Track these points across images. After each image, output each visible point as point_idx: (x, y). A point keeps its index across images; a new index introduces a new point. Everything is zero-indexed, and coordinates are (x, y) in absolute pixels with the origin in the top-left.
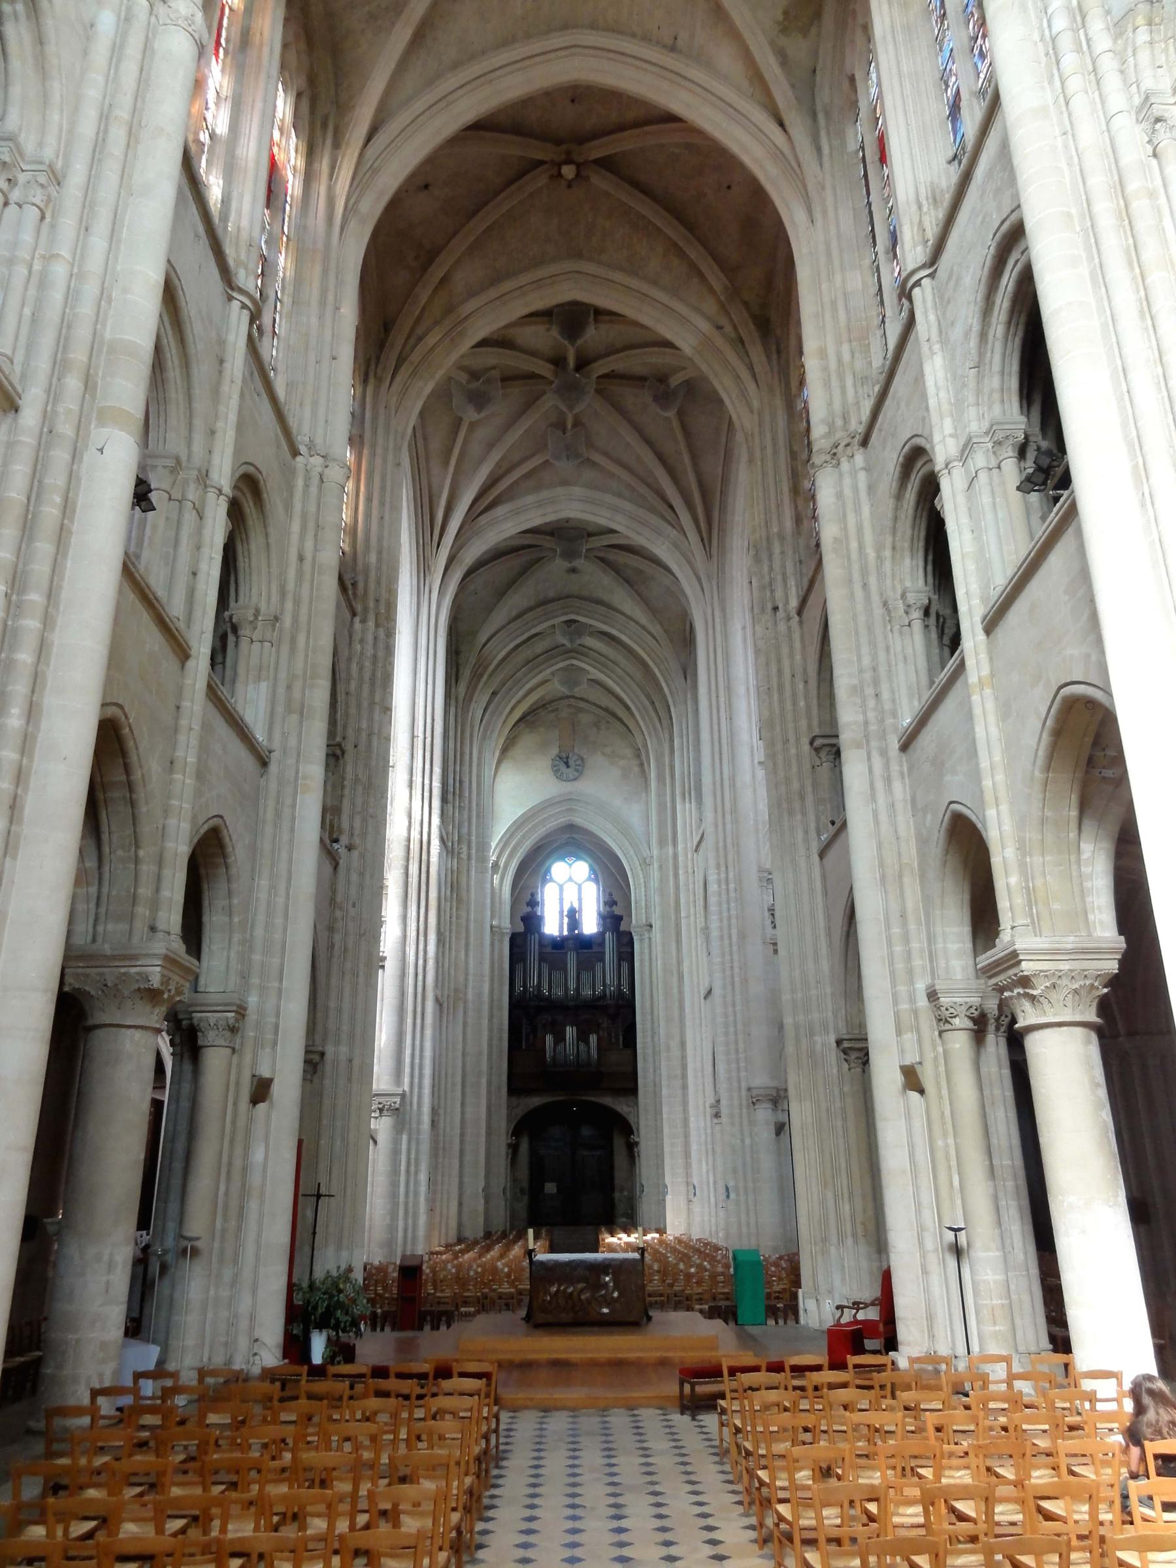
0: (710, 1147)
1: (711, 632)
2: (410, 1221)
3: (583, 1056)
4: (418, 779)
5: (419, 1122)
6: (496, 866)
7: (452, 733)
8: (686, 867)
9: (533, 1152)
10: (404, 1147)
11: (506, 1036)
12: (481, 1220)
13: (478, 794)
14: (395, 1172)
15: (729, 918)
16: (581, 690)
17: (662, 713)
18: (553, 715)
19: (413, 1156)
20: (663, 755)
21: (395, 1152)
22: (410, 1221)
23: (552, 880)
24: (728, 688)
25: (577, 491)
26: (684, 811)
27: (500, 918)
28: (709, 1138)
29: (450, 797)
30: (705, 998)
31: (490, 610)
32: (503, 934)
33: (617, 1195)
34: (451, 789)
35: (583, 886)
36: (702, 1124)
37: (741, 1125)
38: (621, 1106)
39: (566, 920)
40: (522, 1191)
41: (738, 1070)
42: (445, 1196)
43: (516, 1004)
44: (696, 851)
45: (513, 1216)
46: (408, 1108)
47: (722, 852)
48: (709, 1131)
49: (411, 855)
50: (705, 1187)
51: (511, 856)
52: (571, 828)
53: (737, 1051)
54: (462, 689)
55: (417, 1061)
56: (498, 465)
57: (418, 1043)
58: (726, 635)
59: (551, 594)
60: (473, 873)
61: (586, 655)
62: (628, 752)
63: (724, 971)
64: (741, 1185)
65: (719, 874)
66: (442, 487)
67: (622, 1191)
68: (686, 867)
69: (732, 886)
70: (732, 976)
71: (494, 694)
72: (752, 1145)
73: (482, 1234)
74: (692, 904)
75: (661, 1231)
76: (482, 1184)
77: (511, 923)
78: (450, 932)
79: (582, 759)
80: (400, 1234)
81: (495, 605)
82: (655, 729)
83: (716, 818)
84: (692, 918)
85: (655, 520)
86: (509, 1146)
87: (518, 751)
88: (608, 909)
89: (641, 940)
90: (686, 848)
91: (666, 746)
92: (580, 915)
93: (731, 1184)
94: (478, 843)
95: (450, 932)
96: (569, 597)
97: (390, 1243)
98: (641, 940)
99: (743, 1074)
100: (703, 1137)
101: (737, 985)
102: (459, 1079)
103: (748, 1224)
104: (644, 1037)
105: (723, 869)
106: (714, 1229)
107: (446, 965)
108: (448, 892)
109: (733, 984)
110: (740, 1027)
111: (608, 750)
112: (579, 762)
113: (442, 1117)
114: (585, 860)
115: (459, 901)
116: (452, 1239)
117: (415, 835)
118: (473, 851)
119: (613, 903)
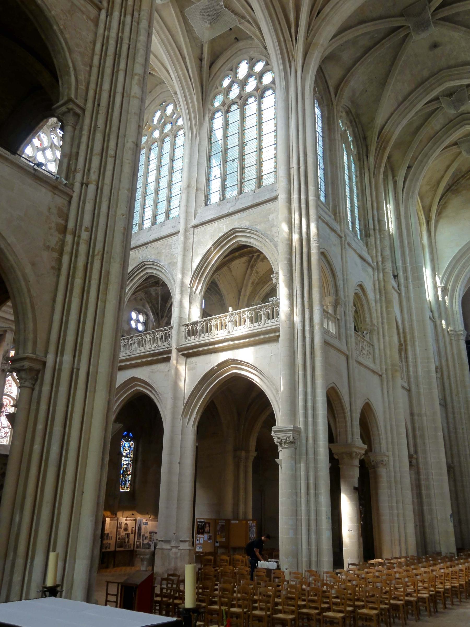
2: (313, 537)
4: (295, 196)
5: (315, 453)
6: (445, 290)
10: (303, 473)
12: (453, 539)
13: (409, 236)
19: (312, 481)
22: (313, 537)
27: (454, 325)
29: (372, 232)
31: (378, 100)
32: (458, 335)
34: (371, 226)
42: (401, 518)
49: (294, 250)
51: (456, 281)
55: (310, 404)
57: (309, 390)
59: (426, 73)
60: (411, 288)
71: (409, 167)
78: (383, 323)
87: (449, 211)
95: (383, 323)
96: (440, 71)
108: (378, 296)
113: (391, 458)
117: (296, 237)
118: (409, 274)
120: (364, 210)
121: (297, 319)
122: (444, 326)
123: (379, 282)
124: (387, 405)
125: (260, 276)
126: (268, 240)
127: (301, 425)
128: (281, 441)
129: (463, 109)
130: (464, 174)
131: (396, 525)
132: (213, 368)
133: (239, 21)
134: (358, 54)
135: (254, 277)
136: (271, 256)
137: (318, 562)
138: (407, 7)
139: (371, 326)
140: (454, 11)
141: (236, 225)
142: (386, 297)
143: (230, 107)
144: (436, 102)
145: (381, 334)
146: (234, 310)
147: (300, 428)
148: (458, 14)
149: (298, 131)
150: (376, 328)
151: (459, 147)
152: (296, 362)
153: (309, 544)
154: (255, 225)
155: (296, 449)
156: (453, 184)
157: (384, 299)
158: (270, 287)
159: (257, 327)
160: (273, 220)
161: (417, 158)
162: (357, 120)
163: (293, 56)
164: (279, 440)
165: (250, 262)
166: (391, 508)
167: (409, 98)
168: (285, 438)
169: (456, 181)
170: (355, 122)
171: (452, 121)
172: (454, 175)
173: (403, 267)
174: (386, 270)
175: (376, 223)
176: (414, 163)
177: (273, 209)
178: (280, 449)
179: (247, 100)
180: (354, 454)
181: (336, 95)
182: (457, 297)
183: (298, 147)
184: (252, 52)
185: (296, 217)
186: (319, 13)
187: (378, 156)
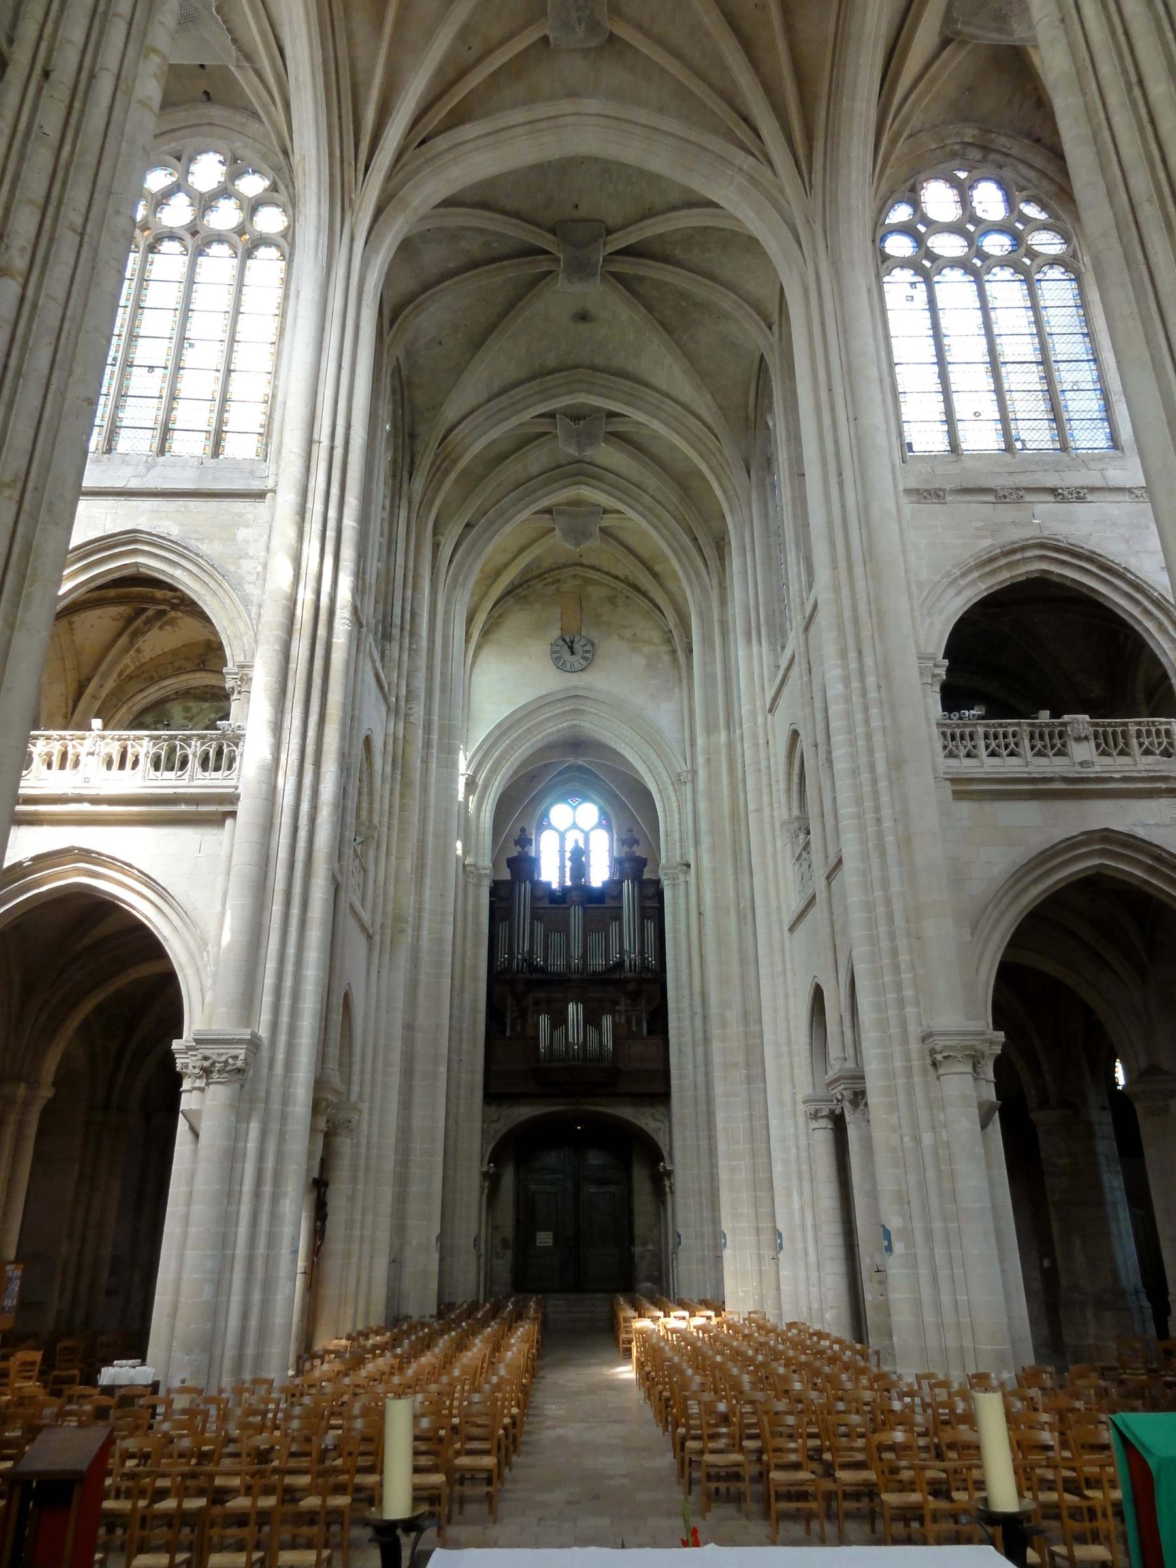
0: (805, 1167)
1: (813, 297)
2: (257, 1297)
3: (593, 1044)
4: (316, 506)
5: (286, 1100)
6: (471, 784)
7: (401, 545)
8: (755, 736)
9: (520, 1187)
10: (252, 1145)
11: (482, 1017)
12: (434, 1286)
13: (445, 659)
14: (228, 1192)
15: (869, 736)
16: (594, 549)
17: (709, 552)
18: (551, 589)
19: (270, 1164)
20: (710, 609)
21: (232, 1156)
22: (257, 1297)
23: (550, 826)
24: (850, 373)
25: (593, 105)
26: (750, 657)
27: (477, 855)
28: (804, 1155)
29: (396, 632)
30: (791, 929)
31: (458, 371)
32: (480, 876)
33: (638, 1250)
35: (592, 835)
36: (792, 1131)
37: (912, 1106)
38: (646, 1120)
39: (568, 864)
40: (505, 1244)
41: (901, 1003)
42: (366, 1247)
43: (497, 978)
44: (770, 711)
45: (490, 1276)
46: (265, 1071)
47: (849, 628)
48: (803, 1142)
49: (297, 626)
50: (799, 1234)
51: (494, 771)
52: (576, 744)
53: (896, 970)
54: (418, 484)
55: (288, 983)
56: (464, 34)
57: (291, 950)
58: (841, 298)
59: (551, 361)
60: (433, 765)
61: (600, 480)
62: (656, 636)
63: (862, 828)
64: (917, 1225)
65: (845, 667)
66: (371, 71)
67: (645, 1243)
68: (755, 736)
69: (871, 680)
70: (880, 835)
71: (469, 526)
72: (935, 1148)
73: (434, 1311)
74: (765, 791)
75: (719, 1309)
76: (437, 1230)
77: (495, 863)
79: (593, 645)
80: (233, 1322)
81: (468, 362)
82: (697, 574)
83: (835, 579)
84: (767, 811)
85: (718, 144)
86: (485, 1175)
87: (503, 633)
88: (626, 849)
89: (674, 886)
90: (753, 712)
91: (714, 595)
92: (588, 858)
93: (894, 1223)
94: (441, 727)
96: (576, 367)
97: (209, 1344)
98: (674, 886)
99: (910, 1010)
100: (794, 1151)
101: (891, 850)
102: (396, 1057)
103: (938, 1307)
104: (679, 1019)
105: (852, 655)
106: (815, 1306)
107: (381, 877)
108: (389, 769)
109: (882, 849)
110: (899, 921)
111: (628, 633)
112: (588, 647)
113: (365, 1116)
114: (594, 802)
115: (406, 784)
116: (377, 1317)
117: (306, 596)
118: (435, 737)
119: (637, 842)
120: (387, 584)
121: (286, 783)
122: (459, 852)
123: (395, 740)
124: (373, 1002)
125: (143, 660)
126: (226, 585)
127: (263, 1032)
128: (213, 1064)
129: (588, 453)
130: (544, 573)
131: (354, 1260)
132: (20, 864)
133: (237, 59)
134: (452, 265)
135: (129, 662)
136: (226, 623)
137: (259, 1358)
138: (565, 222)
139: (368, 828)
140: (641, 272)
141: (143, 523)
142: (402, 774)
143: (159, 239)
144: (547, 420)
145: (384, 848)
146: (105, 728)
147: (260, 1038)
148: (640, 279)
149: (340, 367)
150: (376, 835)
151: (553, 519)
152: (269, 883)
153: (245, 1315)
154: (197, 539)
155: (242, 1086)
156: (521, 585)
157: (399, 778)
158: (163, 691)
159: (168, 782)
160: (247, 542)
161: (485, 513)
162: (406, 393)
163: (351, 200)
164: (206, 1064)
165: (130, 620)
166: (350, 1224)
167: (513, 392)
168: (223, 1059)
169: (527, 581)
170: (402, 395)
171: (560, 466)
172: (526, 570)
173: (424, 720)
174: (412, 719)
175: (408, 616)
176: (479, 520)
177: (250, 516)
178: (186, 1084)
179: (209, 244)
180: (324, 1104)
181: (392, 324)
182: (490, 802)
183: (336, 402)
184: (238, 144)
185: (311, 549)
186: (423, 142)
187: (431, 481)
